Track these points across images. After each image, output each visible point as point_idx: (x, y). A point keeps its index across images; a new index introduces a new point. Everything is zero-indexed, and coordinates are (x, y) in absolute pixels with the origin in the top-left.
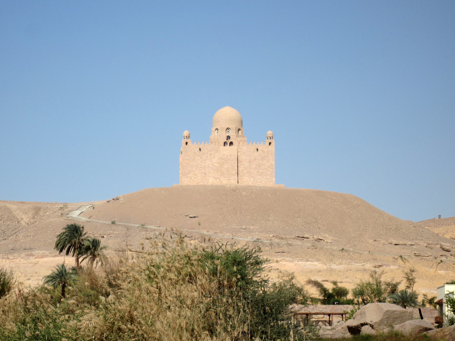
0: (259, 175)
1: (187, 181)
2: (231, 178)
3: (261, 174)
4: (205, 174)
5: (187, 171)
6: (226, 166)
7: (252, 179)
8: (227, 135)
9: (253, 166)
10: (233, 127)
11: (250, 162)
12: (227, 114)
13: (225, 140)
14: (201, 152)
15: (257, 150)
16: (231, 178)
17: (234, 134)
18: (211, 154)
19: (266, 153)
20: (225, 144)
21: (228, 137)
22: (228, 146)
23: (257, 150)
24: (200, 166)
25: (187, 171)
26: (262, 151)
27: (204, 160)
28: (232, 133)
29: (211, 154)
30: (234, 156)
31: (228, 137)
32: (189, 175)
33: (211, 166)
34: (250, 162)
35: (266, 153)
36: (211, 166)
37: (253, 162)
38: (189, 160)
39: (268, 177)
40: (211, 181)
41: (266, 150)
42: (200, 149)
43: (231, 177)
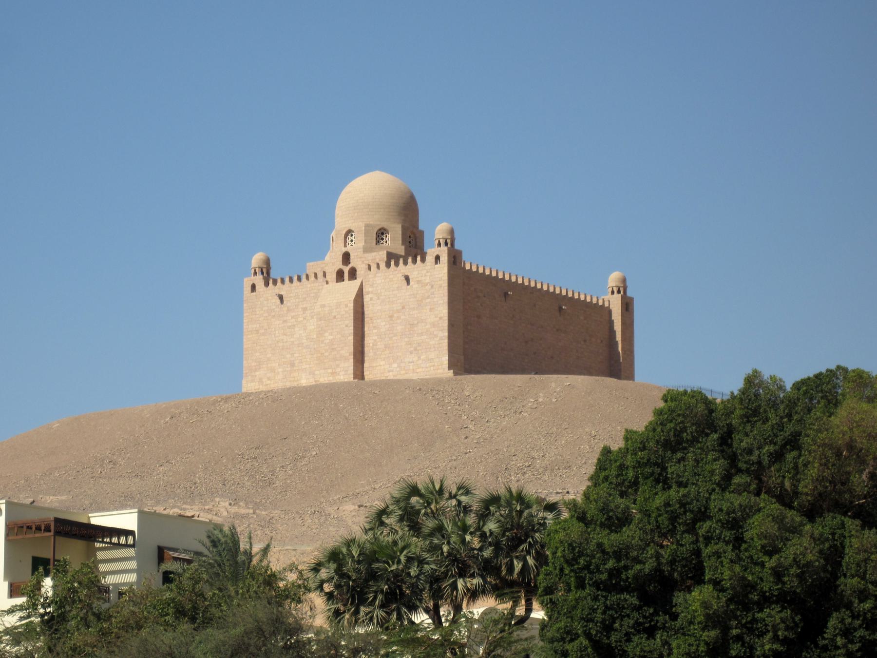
0: (411, 353)
1: (249, 386)
2: (338, 370)
3: (416, 349)
4: (292, 365)
5: (255, 364)
6: (328, 337)
7: (395, 365)
8: (344, 250)
9: (399, 328)
10: (358, 226)
11: (391, 317)
12: (364, 194)
13: (339, 265)
14: (284, 308)
15: (407, 279)
16: (338, 370)
17: (361, 244)
18: (305, 309)
19: (429, 287)
20: (340, 276)
21: (346, 258)
22: (347, 282)
23: (407, 279)
24: (281, 344)
25: (255, 364)
26: (418, 282)
27: (289, 327)
28: (356, 248)
29: (305, 309)
30: (346, 306)
31: (346, 258)
32: (257, 373)
33: (304, 341)
35: (429, 287)
36: (304, 341)
37: (399, 318)
38: (257, 332)
39: (432, 355)
40: (305, 381)
41: (428, 280)
42: (281, 298)
43: (338, 366)
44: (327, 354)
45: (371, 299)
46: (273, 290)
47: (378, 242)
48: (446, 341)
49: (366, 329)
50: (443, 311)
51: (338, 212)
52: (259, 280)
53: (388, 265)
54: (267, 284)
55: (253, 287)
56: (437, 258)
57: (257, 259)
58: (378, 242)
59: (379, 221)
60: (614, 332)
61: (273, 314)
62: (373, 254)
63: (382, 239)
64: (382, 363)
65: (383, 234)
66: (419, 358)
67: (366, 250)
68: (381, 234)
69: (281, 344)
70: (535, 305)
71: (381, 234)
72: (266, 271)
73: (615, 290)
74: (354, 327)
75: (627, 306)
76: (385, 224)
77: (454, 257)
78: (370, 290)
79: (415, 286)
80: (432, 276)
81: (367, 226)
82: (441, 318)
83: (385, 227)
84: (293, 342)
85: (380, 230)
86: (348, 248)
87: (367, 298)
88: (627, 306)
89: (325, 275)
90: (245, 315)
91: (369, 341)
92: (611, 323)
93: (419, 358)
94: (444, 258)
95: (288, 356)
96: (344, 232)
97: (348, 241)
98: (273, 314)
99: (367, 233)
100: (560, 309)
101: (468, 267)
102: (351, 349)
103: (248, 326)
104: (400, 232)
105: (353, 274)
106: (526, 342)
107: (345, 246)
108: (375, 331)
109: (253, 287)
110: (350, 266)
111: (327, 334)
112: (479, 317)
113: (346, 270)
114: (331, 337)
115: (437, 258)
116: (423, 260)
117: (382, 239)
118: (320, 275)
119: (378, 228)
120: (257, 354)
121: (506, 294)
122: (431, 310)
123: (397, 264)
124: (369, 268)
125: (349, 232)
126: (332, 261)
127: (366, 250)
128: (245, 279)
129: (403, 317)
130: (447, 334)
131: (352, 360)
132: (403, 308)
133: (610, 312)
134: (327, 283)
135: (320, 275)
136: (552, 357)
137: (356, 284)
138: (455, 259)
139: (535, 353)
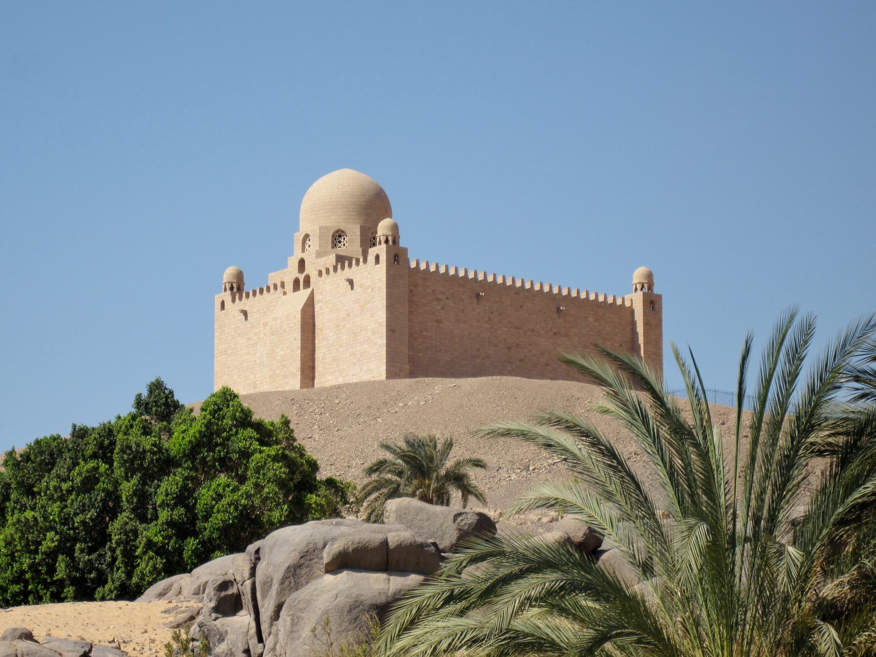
0: (355, 364)
3: (359, 360)
11: (337, 326)
12: (328, 194)
15: (351, 282)
18: (265, 324)
19: (370, 290)
20: (296, 284)
21: (302, 264)
23: (351, 282)
24: (245, 365)
26: (361, 286)
30: (295, 317)
31: (302, 264)
34: (337, 326)
35: (370, 290)
42: (245, 313)
44: (278, 372)
45: (321, 309)
46: (240, 305)
47: (334, 246)
48: (385, 348)
49: (316, 342)
50: (381, 315)
51: (301, 216)
52: (227, 296)
53: (335, 269)
54: (234, 301)
55: (223, 304)
56: (377, 258)
57: (228, 274)
58: (334, 246)
59: (334, 222)
60: (637, 334)
61: (239, 332)
62: (324, 259)
63: (340, 242)
64: (330, 378)
65: (340, 236)
66: (361, 369)
67: (319, 254)
68: (338, 236)
69: (245, 365)
70: (521, 307)
71: (338, 236)
72: (238, 288)
73: (639, 287)
74: (302, 340)
75: (652, 304)
76: (342, 226)
77: (396, 256)
78: (320, 298)
79: (359, 290)
80: (373, 276)
81: (321, 228)
82: (380, 323)
83: (344, 229)
84: (255, 361)
85: (337, 231)
86: (304, 255)
87: (317, 307)
88: (652, 304)
89: (283, 285)
90: (216, 335)
91: (319, 355)
92: (633, 324)
93: (361, 369)
94: (383, 258)
95: (252, 377)
96: (302, 238)
97: (307, 247)
98: (239, 332)
99: (321, 236)
100: (558, 310)
101: (413, 265)
102: (298, 364)
103: (218, 347)
104: (359, 233)
105: (307, 282)
106: (509, 348)
107: (303, 251)
108: (324, 343)
109: (223, 304)
110: (305, 274)
111: (278, 350)
112: (439, 321)
113: (302, 278)
114: (282, 353)
115: (377, 258)
116: (365, 261)
117: (340, 242)
118: (279, 285)
119: (334, 230)
120: (226, 377)
121: (478, 295)
122: (372, 315)
123: (343, 268)
124: (320, 274)
125: (307, 236)
126: (291, 273)
127: (319, 254)
128: (216, 296)
129: (348, 326)
130: (385, 341)
131: (299, 377)
132: (348, 315)
133: (632, 312)
134: (285, 293)
135: (279, 285)
136: (547, 365)
137: (309, 291)
138: (397, 257)
139: (521, 360)
